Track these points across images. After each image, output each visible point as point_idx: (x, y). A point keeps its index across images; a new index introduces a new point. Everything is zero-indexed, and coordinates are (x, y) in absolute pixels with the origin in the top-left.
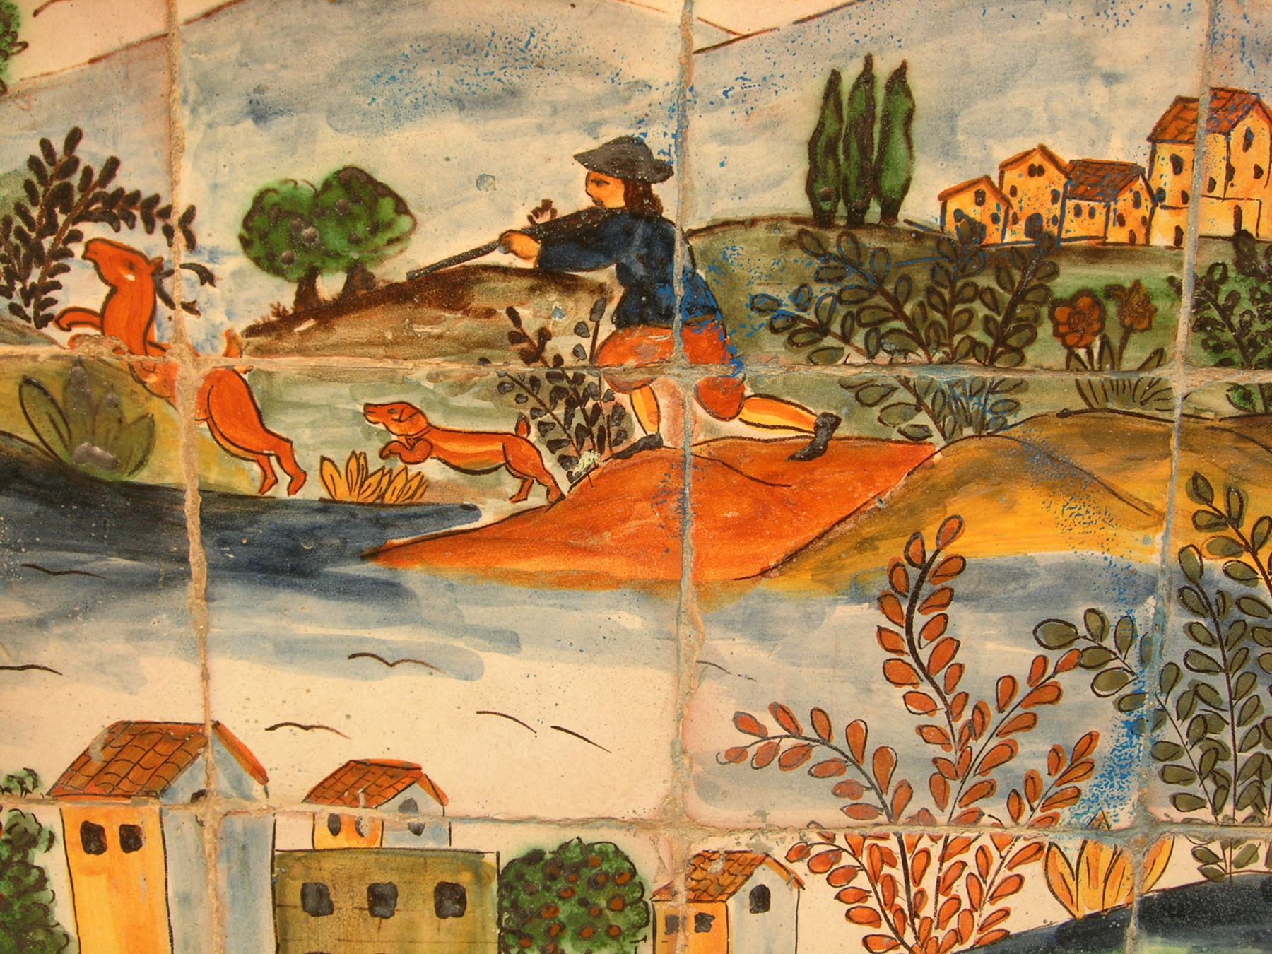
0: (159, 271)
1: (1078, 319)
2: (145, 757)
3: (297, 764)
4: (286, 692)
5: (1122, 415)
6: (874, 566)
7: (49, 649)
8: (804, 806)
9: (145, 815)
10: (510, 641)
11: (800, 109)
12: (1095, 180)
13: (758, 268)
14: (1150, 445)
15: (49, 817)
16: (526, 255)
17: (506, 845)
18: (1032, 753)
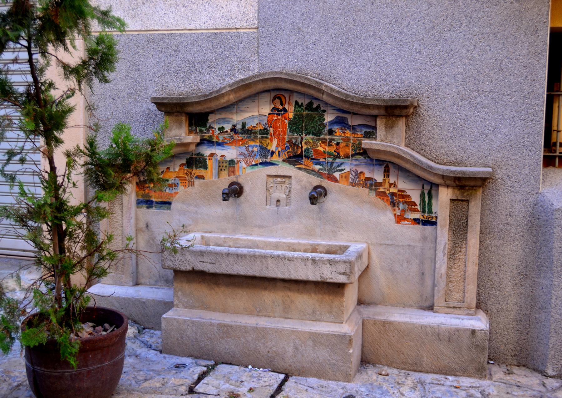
1: (254, 133)
2: (212, 155)
3: (219, 155)
4: (219, 151)
5: (256, 138)
8: (243, 157)
11: (241, 124)
12: (254, 127)
13: (240, 131)
17: (229, 159)
18: (253, 155)
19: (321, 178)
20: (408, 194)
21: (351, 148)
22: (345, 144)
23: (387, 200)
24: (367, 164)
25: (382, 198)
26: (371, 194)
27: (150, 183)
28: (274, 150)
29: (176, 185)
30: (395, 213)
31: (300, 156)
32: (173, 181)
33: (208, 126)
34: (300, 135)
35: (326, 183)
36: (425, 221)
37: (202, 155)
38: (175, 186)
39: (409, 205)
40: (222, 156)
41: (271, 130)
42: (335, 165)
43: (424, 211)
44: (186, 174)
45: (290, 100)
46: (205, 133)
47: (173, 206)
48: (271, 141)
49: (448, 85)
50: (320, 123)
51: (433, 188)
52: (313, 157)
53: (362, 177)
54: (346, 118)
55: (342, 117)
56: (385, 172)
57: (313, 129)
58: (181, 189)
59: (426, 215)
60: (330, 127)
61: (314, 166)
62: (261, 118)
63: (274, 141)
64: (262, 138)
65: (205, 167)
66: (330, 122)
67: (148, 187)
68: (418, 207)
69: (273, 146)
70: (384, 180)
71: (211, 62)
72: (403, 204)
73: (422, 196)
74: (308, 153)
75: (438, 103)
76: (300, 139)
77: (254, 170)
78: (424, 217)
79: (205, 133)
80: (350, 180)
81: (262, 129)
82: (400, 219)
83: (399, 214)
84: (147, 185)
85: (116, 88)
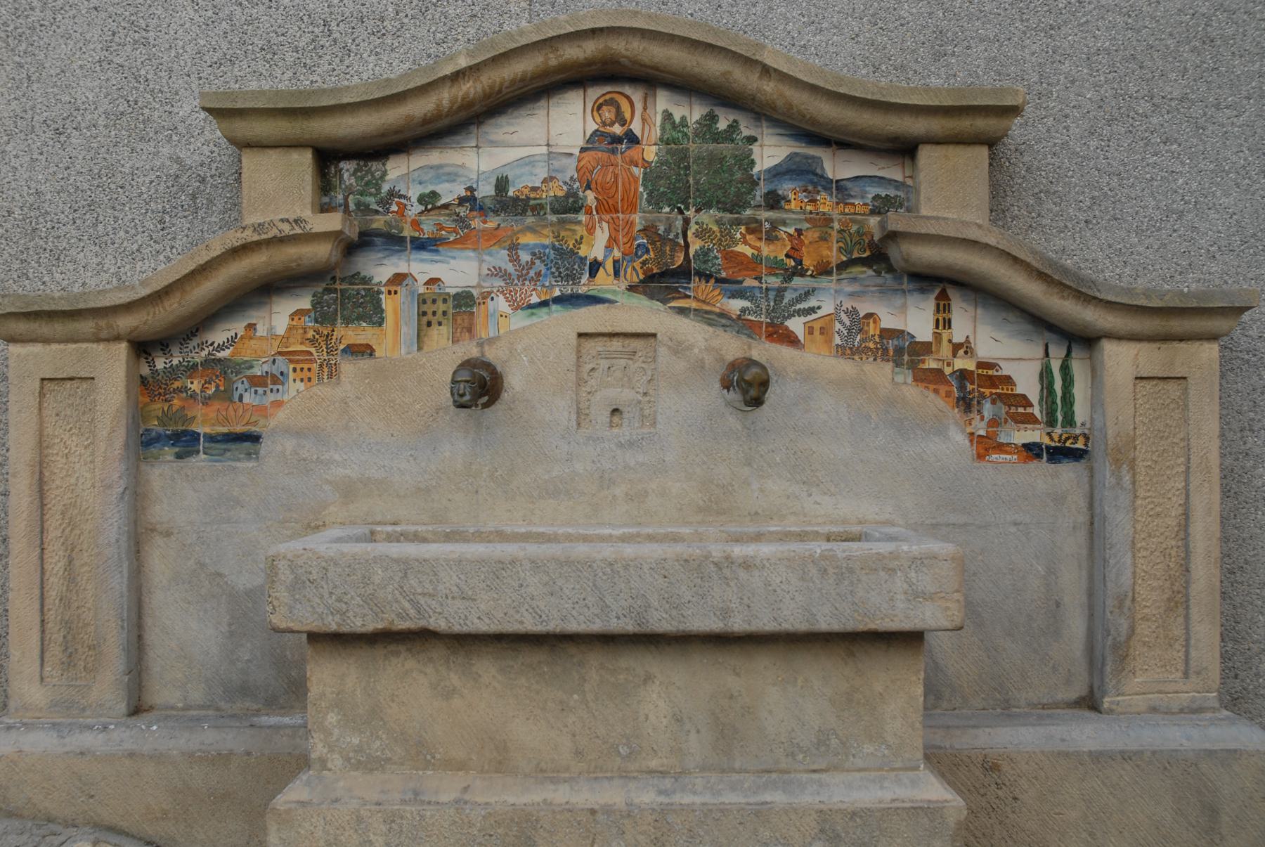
0: (405, 205)
2: (399, 279)
3: (422, 279)
4: (420, 268)
6: (507, 244)
7: (385, 262)
8: (499, 283)
9: (398, 289)
10: (454, 258)
12: (534, 189)
13: (488, 203)
14: (546, 226)
15: (383, 289)
16: (456, 202)
17: (453, 291)
18: (532, 273)
19: (750, 336)
21: (835, 246)
22: (816, 235)
23: (948, 394)
24: (884, 291)
25: (932, 387)
26: (899, 379)
27: (190, 377)
28: (600, 258)
29: (278, 379)
30: (969, 430)
31: (684, 273)
32: (266, 368)
33: (385, 188)
34: (681, 212)
35: (763, 351)
36: (1055, 448)
37: (366, 281)
38: (275, 380)
39: (1009, 406)
40: (433, 281)
41: (590, 196)
42: (789, 296)
43: (1051, 422)
44: (312, 341)
45: (645, 109)
46: (377, 212)
47: (265, 446)
48: (591, 230)
49: (1073, 82)
50: (738, 175)
51: (1073, 354)
52: (724, 275)
53: (872, 330)
54: (818, 160)
55: (807, 157)
56: (938, 311)
57: (719, 193)
58: (294, 388)
59: (1058, 430)
60: (771, 187)
61: (725, 300)
62: (556, 164)
63: (598, 230)
64: (562, 222)
65: (374, 315)
66: (769, 171)
67: (184, 389)
68: (1036, 411)
69: (596, 248)
70: (937, 336)
71: (382, 19)
72: (993, 402)
73: (1045, 376)
74: (706, 262)
75: (1048, 131)
76: (679, 223)
77: (535, 320)
78: (1052, 439)
79: (377, 212)
80: (837, 340)
81: (560, 194)
82: (986, 446)
83: (982, 433)
84: (177, 384)
85: (68, 99)
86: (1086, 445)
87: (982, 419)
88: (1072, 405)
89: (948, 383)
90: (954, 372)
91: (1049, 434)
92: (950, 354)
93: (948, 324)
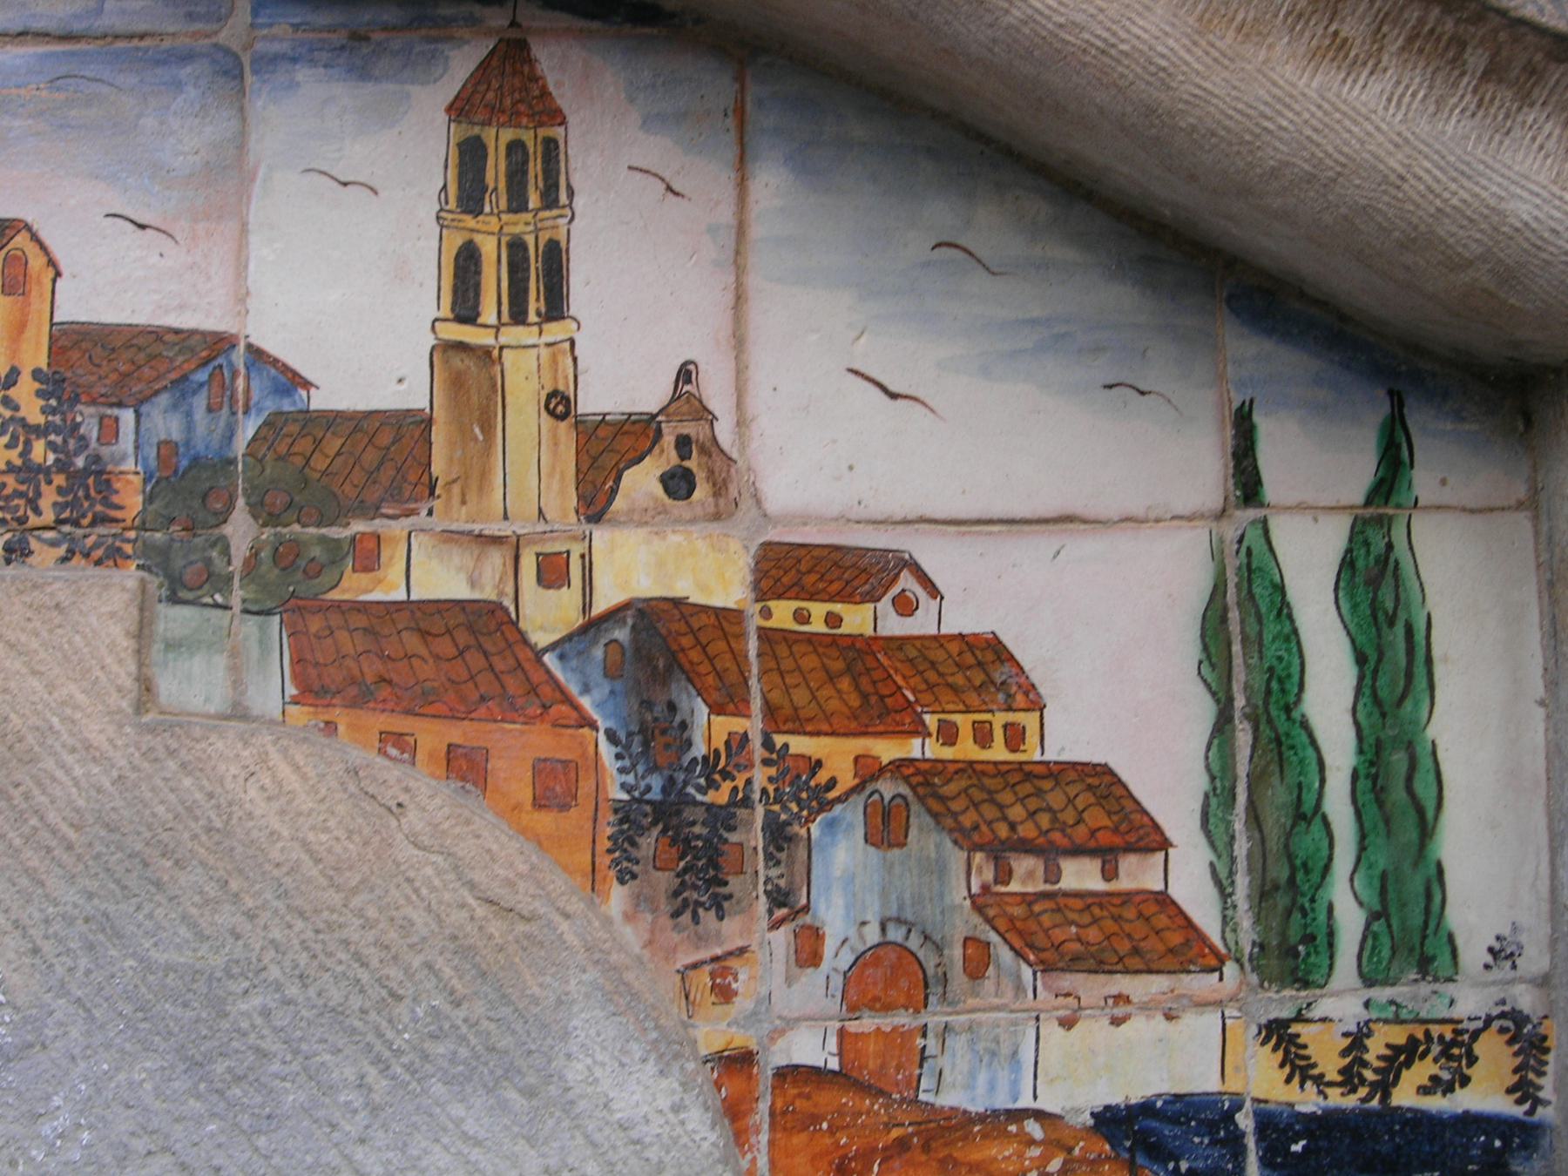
20: (960, 619)
23: (554, 787)
25: (432, 735)
26: (193, 684)
30: (715, 1031)
36: (1322, 1126)
39: (1000, 853)
43: (1293, 954)
51: (1423, 481)
56: (470, 194)
59: (1341, 1003)
70: (467, 371)
72: (885, 829)
73: (1242, 628)
78: (1298, 1067)
83: (811, 1048)
86: (1523, 1090)
87: (808, 951)
88: (1426, 830)
89: (548, 702)
90: (593, 626)
91: (1278, 1033)
92: (562, 500)
93: (542, 282)
